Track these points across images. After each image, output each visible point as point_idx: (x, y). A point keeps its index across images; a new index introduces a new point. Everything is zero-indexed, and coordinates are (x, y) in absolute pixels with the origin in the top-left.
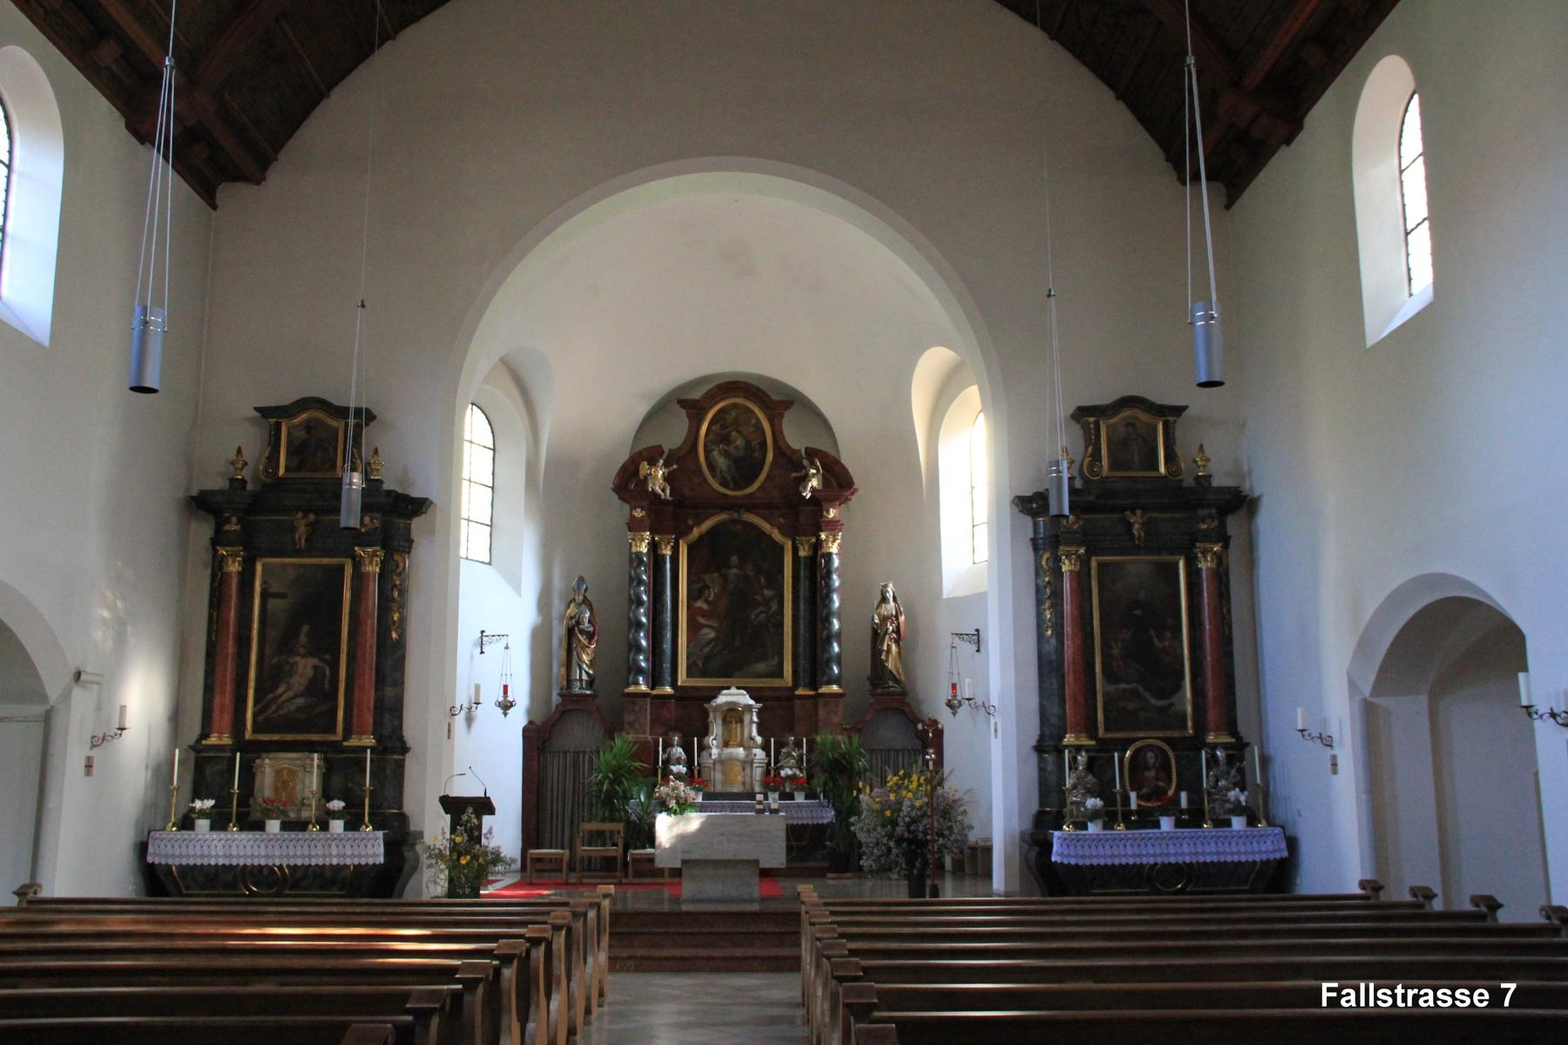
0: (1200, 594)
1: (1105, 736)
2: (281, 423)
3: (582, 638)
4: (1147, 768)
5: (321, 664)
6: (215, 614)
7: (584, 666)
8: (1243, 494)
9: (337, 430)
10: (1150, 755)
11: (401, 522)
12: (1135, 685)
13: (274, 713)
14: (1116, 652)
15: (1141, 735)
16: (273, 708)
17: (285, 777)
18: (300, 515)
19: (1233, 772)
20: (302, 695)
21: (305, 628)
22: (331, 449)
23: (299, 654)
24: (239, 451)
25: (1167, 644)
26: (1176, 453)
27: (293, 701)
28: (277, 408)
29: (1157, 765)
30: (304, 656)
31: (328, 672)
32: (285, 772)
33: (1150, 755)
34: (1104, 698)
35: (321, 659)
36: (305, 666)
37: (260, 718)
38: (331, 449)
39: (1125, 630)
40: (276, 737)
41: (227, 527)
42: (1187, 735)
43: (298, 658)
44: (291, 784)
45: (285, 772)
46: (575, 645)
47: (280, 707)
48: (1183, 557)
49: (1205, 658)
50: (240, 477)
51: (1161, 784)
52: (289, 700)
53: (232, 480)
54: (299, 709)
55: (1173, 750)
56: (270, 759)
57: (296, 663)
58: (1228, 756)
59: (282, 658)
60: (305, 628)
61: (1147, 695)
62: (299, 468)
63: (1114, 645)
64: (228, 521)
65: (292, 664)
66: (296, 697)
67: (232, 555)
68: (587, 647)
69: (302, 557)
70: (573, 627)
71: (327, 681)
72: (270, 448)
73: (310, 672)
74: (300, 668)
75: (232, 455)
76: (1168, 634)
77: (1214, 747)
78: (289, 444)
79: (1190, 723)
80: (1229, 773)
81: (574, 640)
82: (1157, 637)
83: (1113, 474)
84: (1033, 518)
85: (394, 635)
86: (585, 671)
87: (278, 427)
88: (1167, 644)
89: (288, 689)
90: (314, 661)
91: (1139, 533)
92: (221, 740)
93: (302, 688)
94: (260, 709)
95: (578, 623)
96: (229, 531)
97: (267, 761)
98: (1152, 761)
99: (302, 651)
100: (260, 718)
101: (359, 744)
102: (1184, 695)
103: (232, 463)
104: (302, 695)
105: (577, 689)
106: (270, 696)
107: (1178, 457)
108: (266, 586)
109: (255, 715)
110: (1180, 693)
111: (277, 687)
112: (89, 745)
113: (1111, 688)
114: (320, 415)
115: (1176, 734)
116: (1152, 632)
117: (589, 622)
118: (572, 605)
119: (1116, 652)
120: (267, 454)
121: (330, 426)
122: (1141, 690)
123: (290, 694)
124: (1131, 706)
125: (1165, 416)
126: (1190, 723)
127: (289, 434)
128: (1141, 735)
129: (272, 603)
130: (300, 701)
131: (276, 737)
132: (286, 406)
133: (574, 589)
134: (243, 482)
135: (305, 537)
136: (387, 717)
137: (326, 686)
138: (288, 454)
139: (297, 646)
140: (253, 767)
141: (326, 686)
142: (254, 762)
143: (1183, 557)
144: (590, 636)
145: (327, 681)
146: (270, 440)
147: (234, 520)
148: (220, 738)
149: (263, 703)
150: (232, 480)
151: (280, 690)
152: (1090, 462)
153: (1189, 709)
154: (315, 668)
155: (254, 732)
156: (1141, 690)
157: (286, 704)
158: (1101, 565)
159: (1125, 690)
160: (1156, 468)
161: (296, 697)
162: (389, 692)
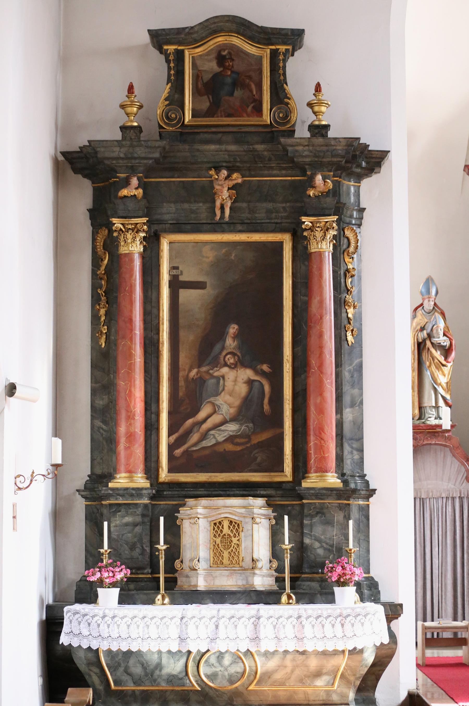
2: (183, 51)
3: (437, 354)
5: (254, 377)
6: (102, 312)
7: (440, 390)
9: (259, 60)
11: (351, 185)
13: (195, 444)
16: (195, 437)
17: (226, 530)
18: (224, 173)
20: (233, 419)
21: (233, 329)
22: (253, 87)
23: (226, 365)
24: (131, 89)
27: (222, 428)
28: (179, 31)
30: (233, 367)
31: (267, 388)
32: (226, 524)
35: (257, 372)
36: (235, 381)
37: (178, 452)
38: (253, 87)
40: (202, 477)
41: (124, 192)
43: (225, 370)
44: (235, 540)
45: (226, 524)
46: (428, 363)
47: (204, 436)
50: (135, 124)
52: (216, 427)
53: (123, 128)
54: (230, 439)
56: (205, 508)
57: (223, 377)
59: (204, 369)
60: (233, 329)
62: (210, 113)
64: (126, 183)
65: (218, 378)
66: (224, 422)
67: (133, 230)
68: (444, 365)
69: (223, 231)
70: (424, 340)
71: (266, 401)
72: (170, 84)
73: (243, 389)
74: (229, 384)
75: (122, 96)
78: (197, 77)
81: (425, 356)
85: (350, 338)
86: (442, 396)
87: (180, 56)
89: (215, 412)
90: (248, 373)
92: (132, 481)
93: (232, 411)
94: (176, 440)
95: (430, 336)
96: (125, 197)
97: (200, 510)
99: (231, 360)
100: (178, 452)
101: (321, 485)
103: (123, 107)
104: (233, 419)
105: (433, 419)
106: (190, 422)
108: (175, 272)
109: (171, 448)
111: (197, 410)
112: (14, 487)
114: (237, 41)
117: (444, 335)
118: (420, 311)
120: (165, 94)
121: (247, 54)
123: (216, 419)
127: (194, 65)
129: (184, 294)
130: (232, 428)
131: (202, 477)
132: (192, 28)
133: (422, 293)
134: (139, 129)
135: (228, 204)
136: (347, 448)
137: (266, 407)
138: (196, 92)
139: (224, 353)
140: (177, 518)
141: (266, 407)
142: (178, 512)
144: (447, 352)
145: (266, 401)
146: (169, 75)
147: (135, 181)
148: (131, 478)
149: (181, 430)
150: (123, 128)
151: (202, 415)
154: (250, 382)
155: (170, 470)
157: (212, 432)
161: (224, 422)
162: (348, 414)
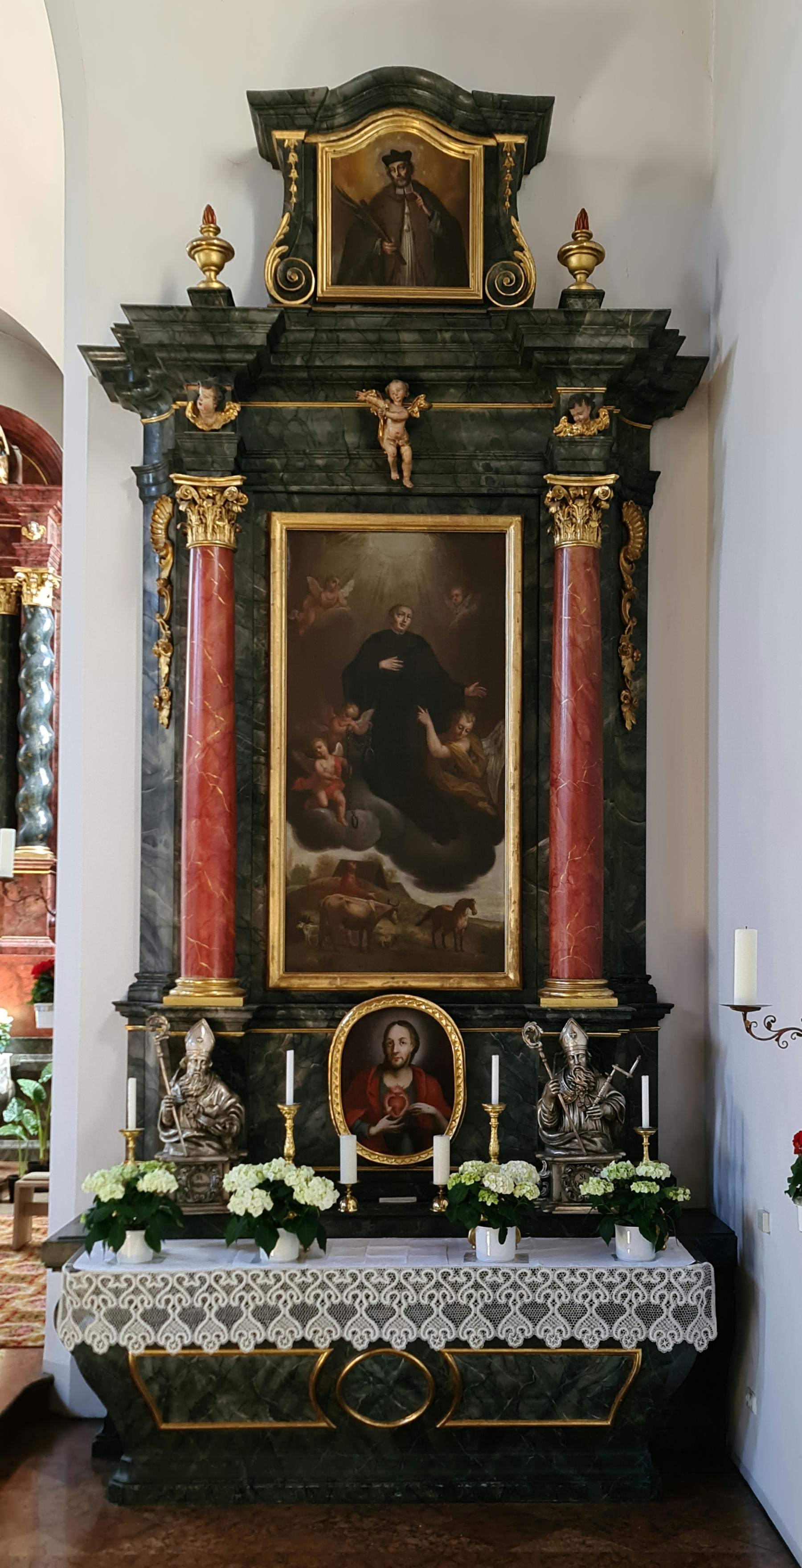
0: (552, 619)
1: (284, 984)
4: (389, 1067)
8: (684, 351)
10: (398, 1033)
12: (372, 851)
14: (326, 765)
15: (376, 982)
19: (603, 1087)
25: (462, 746)
26: (515, 237)
29: (418, 1056)
33: (398, 1033)
34: (287, 884)
39: (353, 710)
42: (503, 984)
48: (518, 519)
49: (554, 783)
51: (427, 1108)
55: (460, 1022)
58: (592, 1044)
61: (402, 877)
63: (322, 746)
76: (466, 723)
77: (560, 1017)
79: (510, 955)
80: (591, 1090)
82: (438, 732)
83: (344, 291)
84: (143, 417)
88: (462, 746)
91: (398, 448)
98: (403, 1050)
102: (501, 883)
107: (521, 249)
110: (490, 875)
113: (310, 859)
115: (468, 982)
116: (425, 717)
119: (326, 765)
122: (387, 864)
124: (358, 907)
125: (489, 133)
126: (510, 955)
128: (376, 982)
143: (518, 519)
152: (282, 257)
153: (511, 917)
156: (387, 864)
158: (292, 534)
159: (344, 865)
160: (465, 283)
